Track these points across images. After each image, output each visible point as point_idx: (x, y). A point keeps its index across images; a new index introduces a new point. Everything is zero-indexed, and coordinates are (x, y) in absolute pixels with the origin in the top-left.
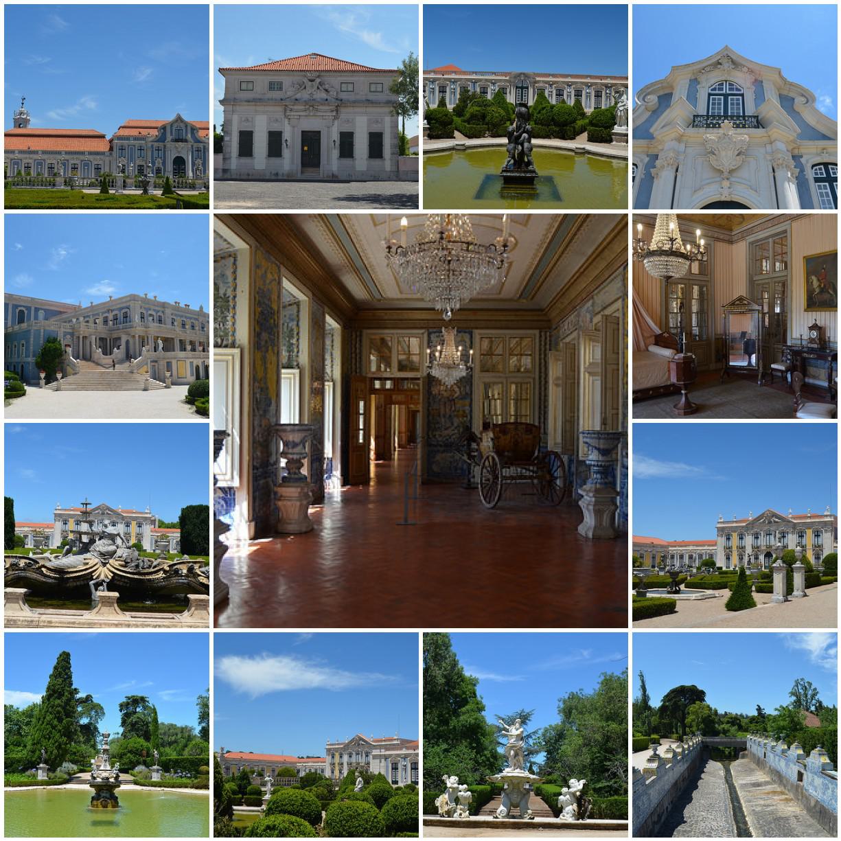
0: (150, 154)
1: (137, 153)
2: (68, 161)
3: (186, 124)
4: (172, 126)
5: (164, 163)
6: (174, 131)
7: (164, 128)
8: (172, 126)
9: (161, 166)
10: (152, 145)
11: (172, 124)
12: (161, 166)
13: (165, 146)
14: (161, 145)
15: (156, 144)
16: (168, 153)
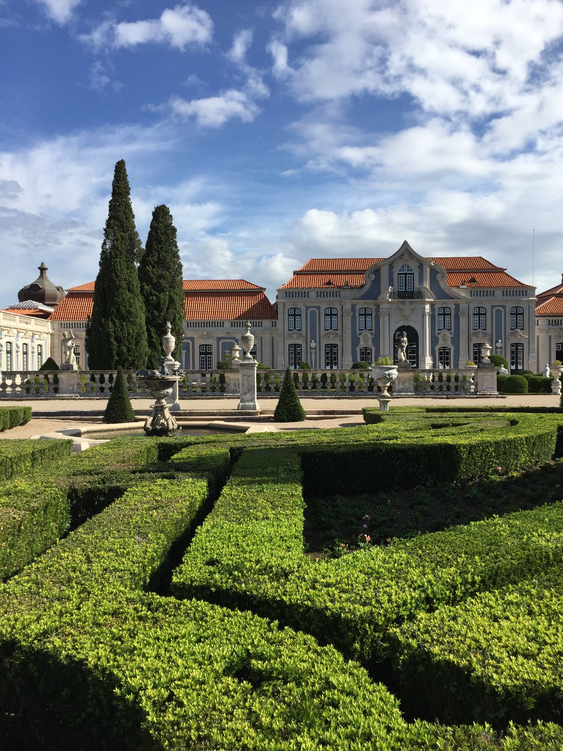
0: (348, 322)
1: (324, 321)
2: (192, 339)
3: (421, 262)
4: (391, 266)
5: (376, 340)
6: (395, 276)
7: (377, 271)
8: (391, 266)
9: (370, 344)
10: (353, 306)
11: (392, 262)
12: (370, 344)
13: (378, 306)
14: (370, 305)
15: (361, 304)
16: (384, 321)
